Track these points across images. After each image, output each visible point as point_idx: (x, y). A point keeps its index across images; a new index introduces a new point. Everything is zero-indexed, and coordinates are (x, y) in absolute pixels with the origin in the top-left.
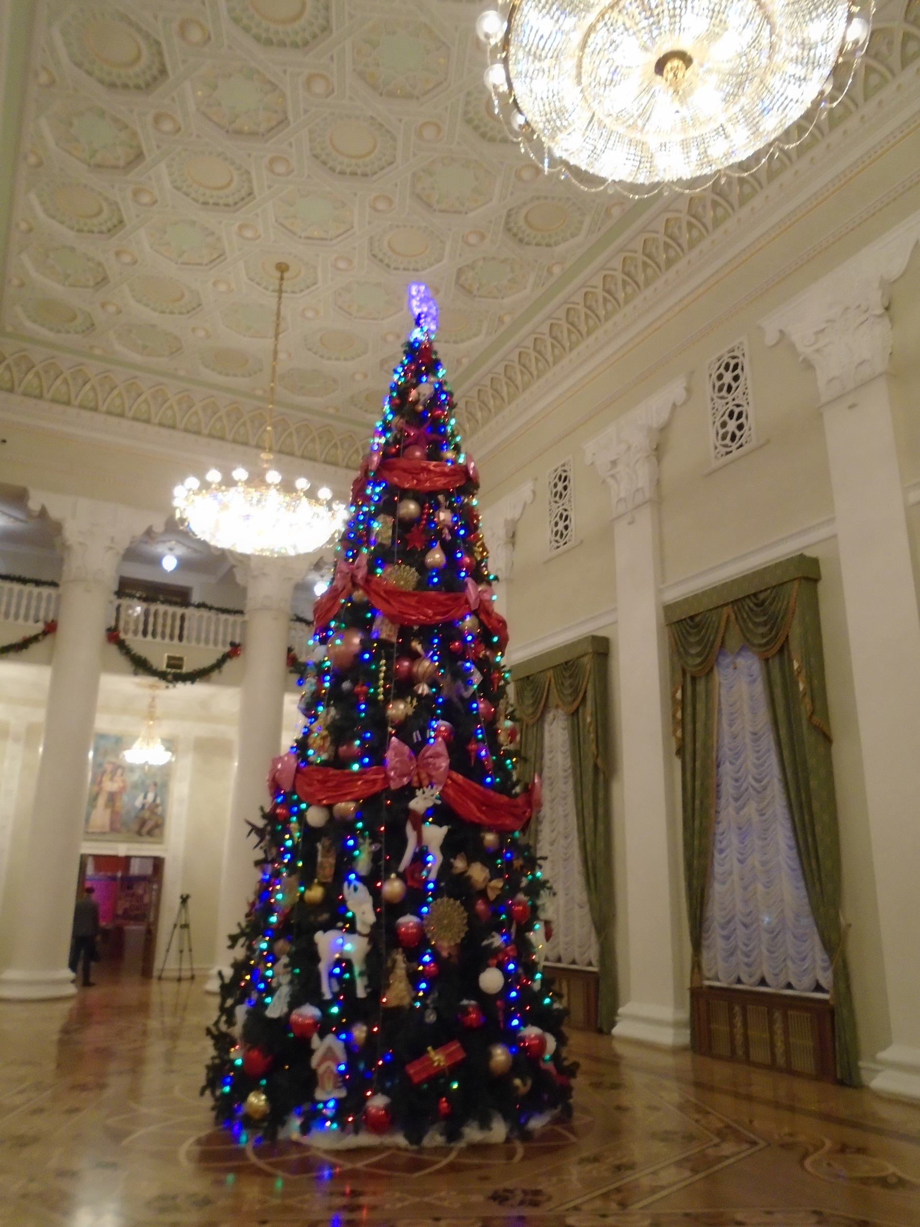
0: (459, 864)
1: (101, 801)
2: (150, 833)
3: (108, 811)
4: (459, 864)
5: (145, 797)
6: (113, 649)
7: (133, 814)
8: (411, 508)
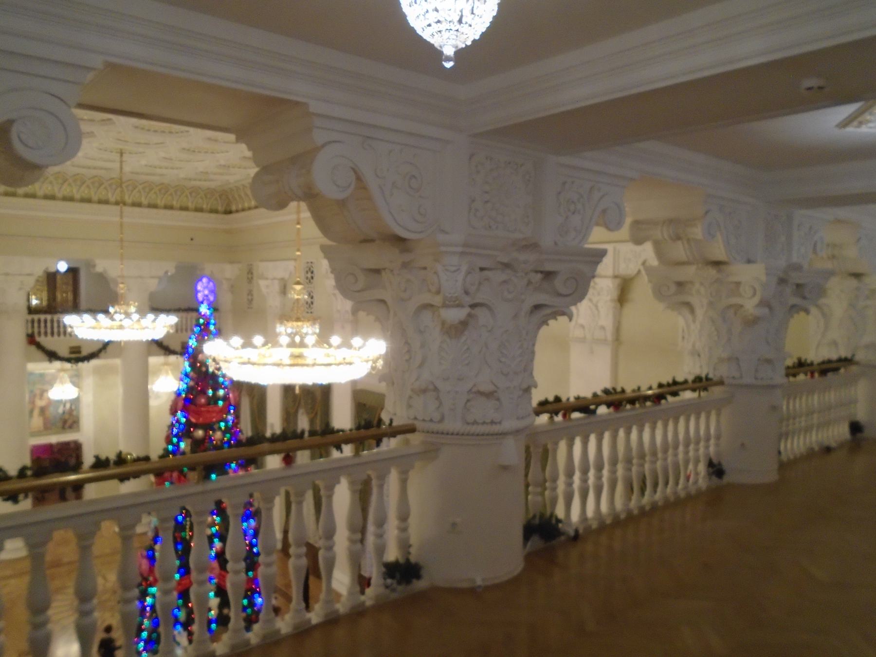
1: (36, 412)
2: (71, 427)
5: (65, 406)
6: (33, 348)
8: (200, 433)
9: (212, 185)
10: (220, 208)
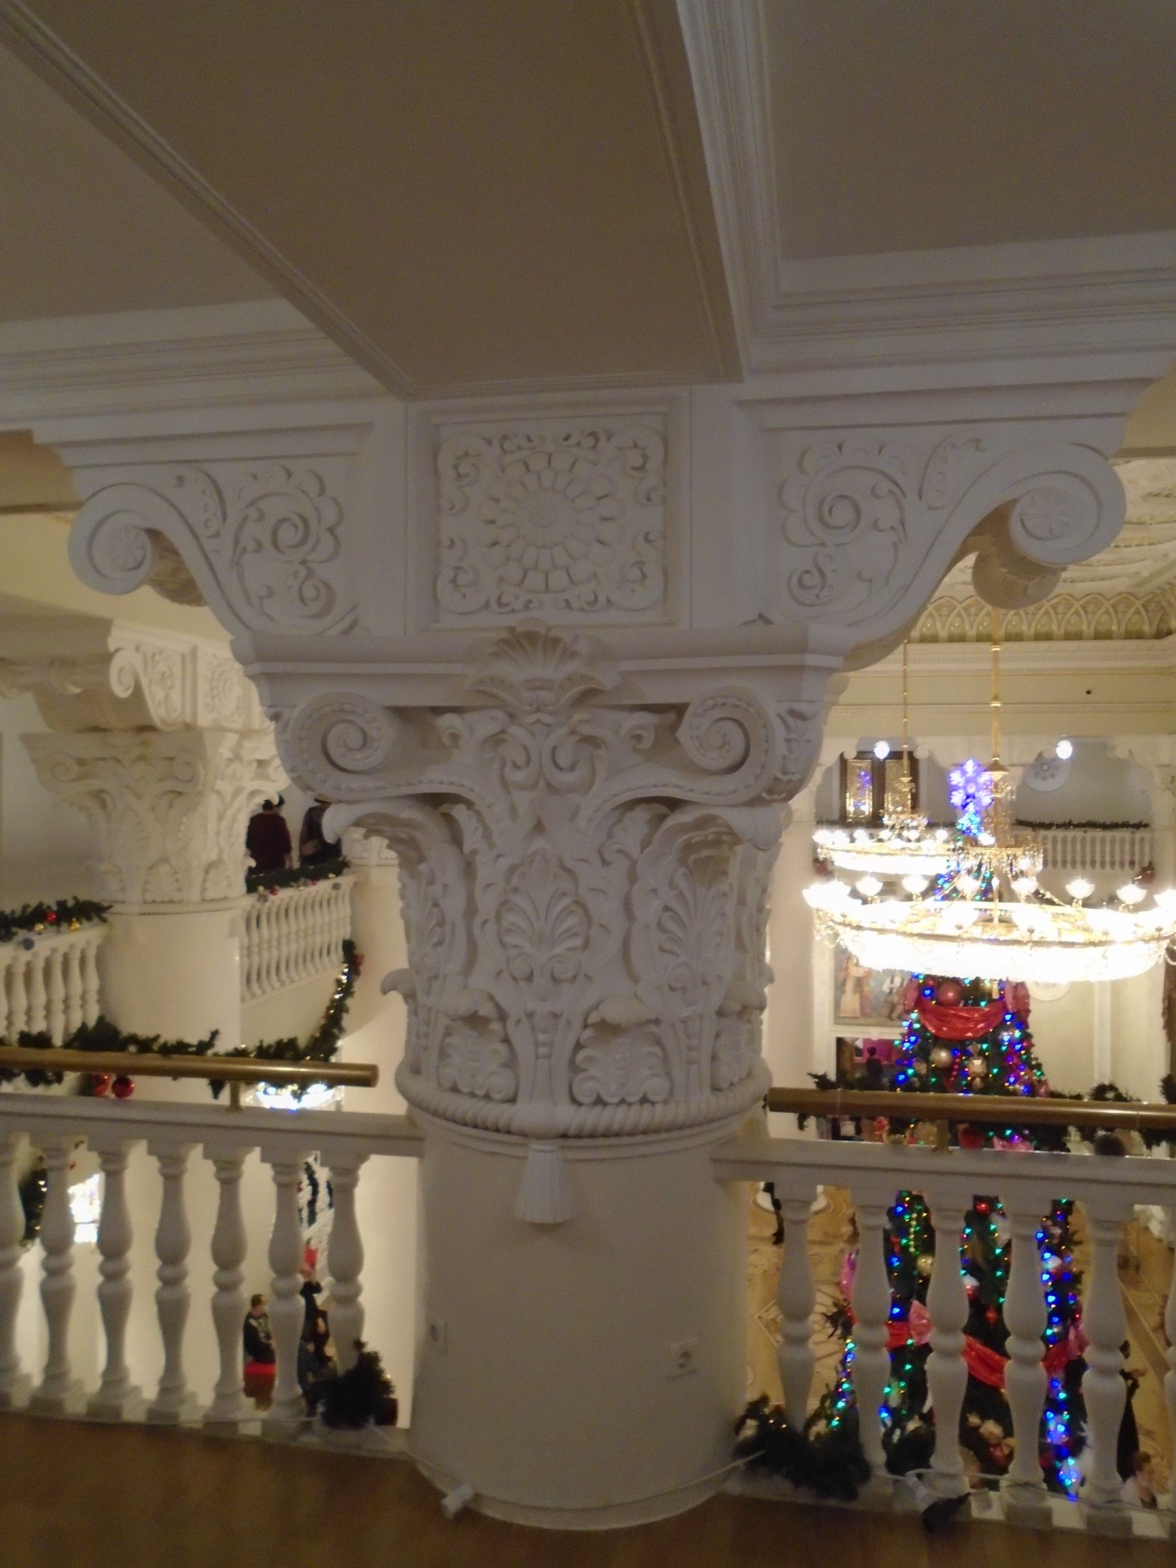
0: (974, 1420)
1: (850, 986)
3: (858, 996)
4: (974, 1420)
5: (892, 982)
7: (882, 999)
8: (943, 1056)
9: (1122, 585)
10: (1146, 628)
